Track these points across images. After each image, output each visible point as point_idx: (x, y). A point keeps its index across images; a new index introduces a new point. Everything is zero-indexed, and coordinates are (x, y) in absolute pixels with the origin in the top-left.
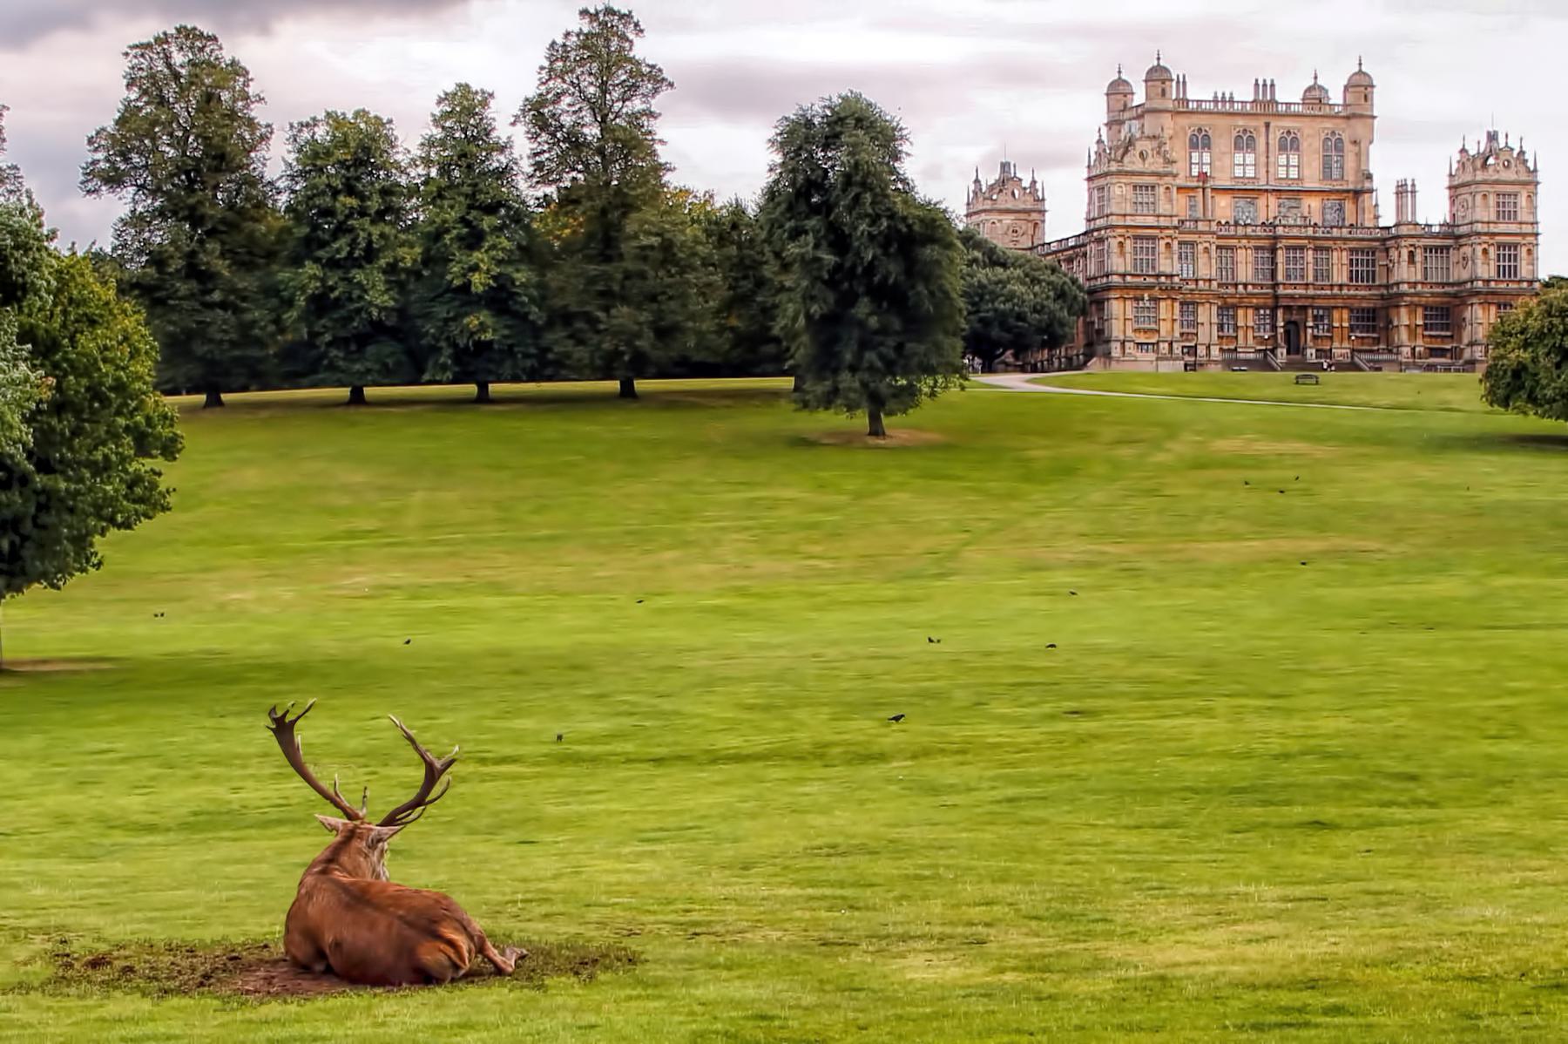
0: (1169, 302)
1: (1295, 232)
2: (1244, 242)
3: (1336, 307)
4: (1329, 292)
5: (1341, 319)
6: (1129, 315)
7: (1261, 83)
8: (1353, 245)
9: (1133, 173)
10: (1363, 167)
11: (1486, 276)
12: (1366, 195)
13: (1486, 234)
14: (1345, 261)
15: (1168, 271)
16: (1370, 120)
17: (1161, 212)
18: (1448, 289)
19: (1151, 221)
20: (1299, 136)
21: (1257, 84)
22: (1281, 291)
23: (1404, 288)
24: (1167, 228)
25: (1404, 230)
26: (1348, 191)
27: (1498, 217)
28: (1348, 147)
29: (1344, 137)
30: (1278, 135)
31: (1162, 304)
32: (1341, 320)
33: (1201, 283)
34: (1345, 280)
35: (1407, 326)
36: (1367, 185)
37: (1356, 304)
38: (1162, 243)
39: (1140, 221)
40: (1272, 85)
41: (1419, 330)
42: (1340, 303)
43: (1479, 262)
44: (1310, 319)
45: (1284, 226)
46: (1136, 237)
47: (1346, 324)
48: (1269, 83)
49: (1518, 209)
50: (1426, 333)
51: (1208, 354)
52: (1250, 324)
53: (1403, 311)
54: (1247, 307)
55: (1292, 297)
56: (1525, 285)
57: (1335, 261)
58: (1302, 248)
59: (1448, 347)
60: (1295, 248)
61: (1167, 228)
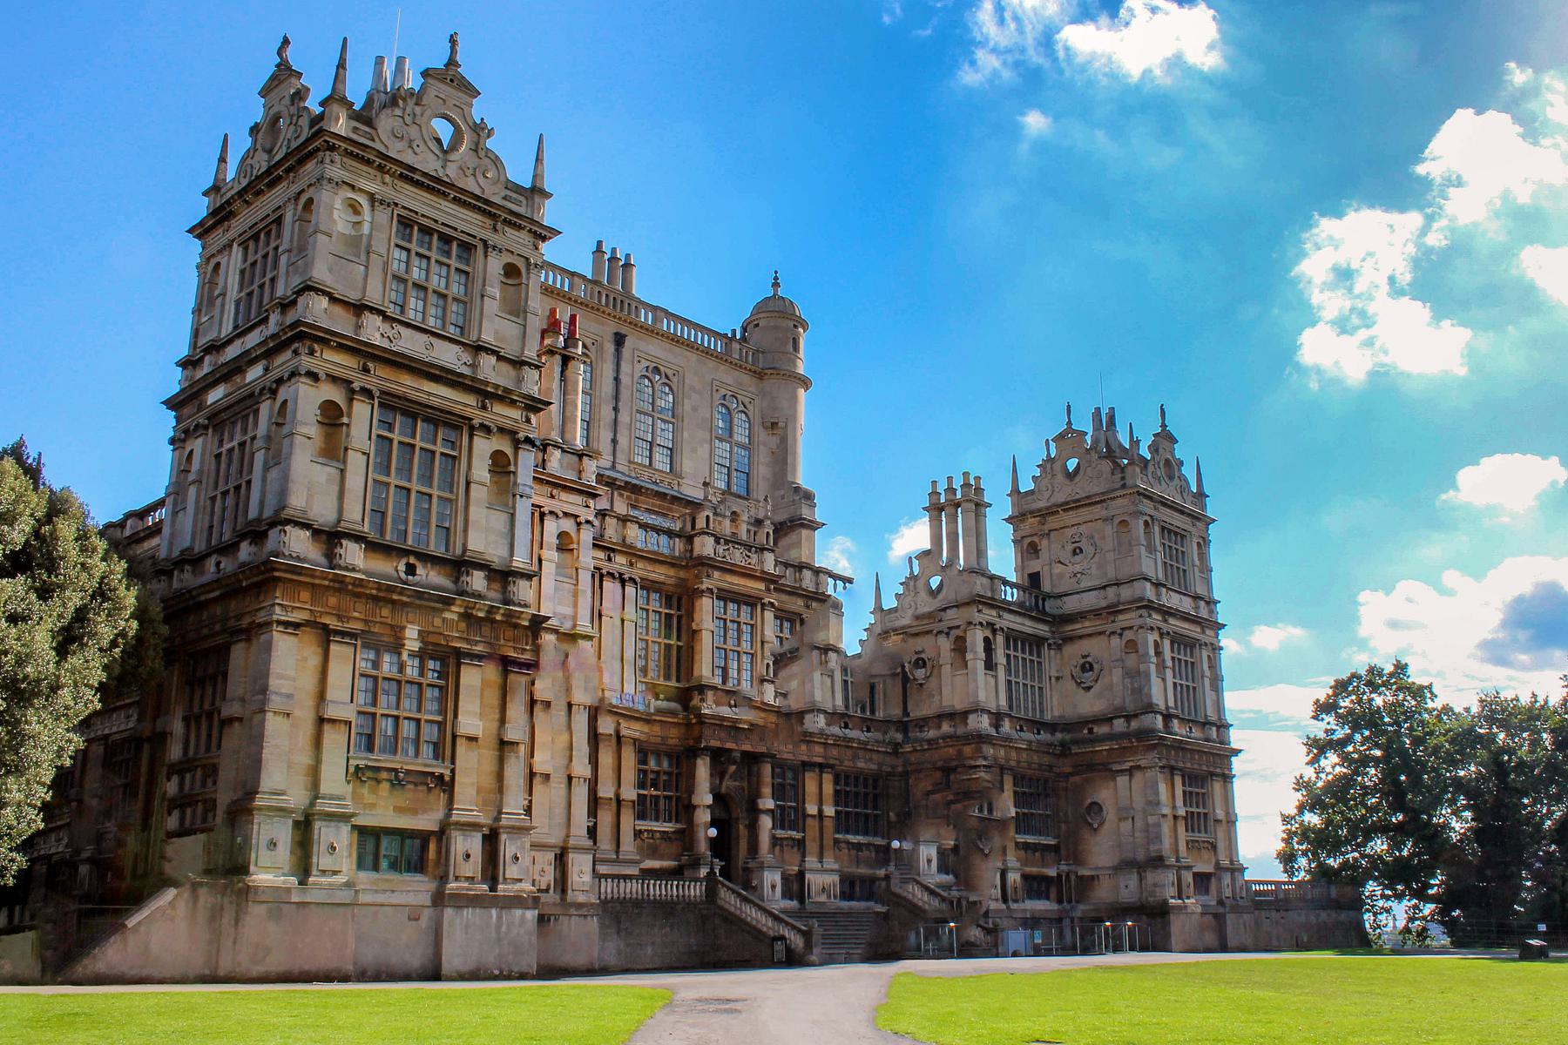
5: (819, 797)
6: (341, 706)
9: (409, 175)
12: (805, 532)
15: (495, 553)
17: (488, 337)
19: (449, 356)
24: (505, 397)
38: (484, 447)
39: (410, 344)
40: (628, 266)
44: (767, 790)
46: (392, 404)
47: (829, 811)
50: (1021, 839)
55: (733, 728)
58: (752, 601)
59: (1052, 872)
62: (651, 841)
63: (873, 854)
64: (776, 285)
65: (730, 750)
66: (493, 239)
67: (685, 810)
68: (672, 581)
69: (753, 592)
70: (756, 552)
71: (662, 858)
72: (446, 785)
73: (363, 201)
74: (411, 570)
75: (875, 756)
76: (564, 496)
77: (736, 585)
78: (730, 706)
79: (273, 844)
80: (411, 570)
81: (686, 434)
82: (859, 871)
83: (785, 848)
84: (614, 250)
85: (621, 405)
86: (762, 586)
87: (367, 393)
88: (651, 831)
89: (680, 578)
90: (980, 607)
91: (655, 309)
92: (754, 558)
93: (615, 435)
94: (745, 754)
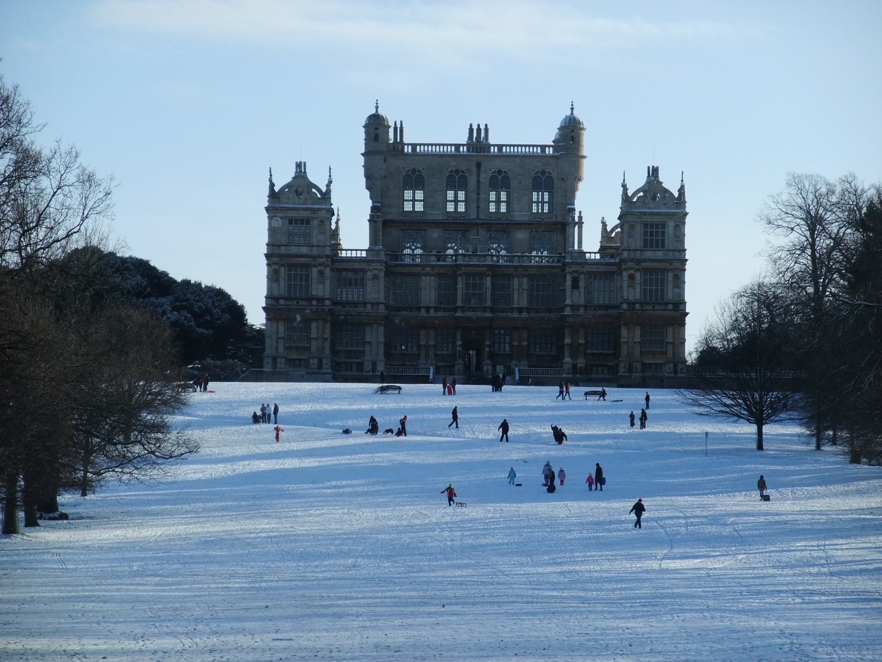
0: (320, 323)
7: (475, 127)
11: (632, 298)
13: (632, 260)
14: (525, 286)
15: (320, 294)
18: (610, 311)
19: (304, 250)
21: (471, 130)
22: (459, 314)
23: (567, 312)
24: (320, 257)
27: (645, 246)
29: (554, 175)
30: (490, 174)
31: (314, 325)
33: (369, 306)
34: (524, 303)
35: (570, 345)
38: (315, 270)
39: (294, 250)
40: (486, 129)
43: (625, 285)
48: (482, 127)
49: (666, 238)
52: (432, 343)
53: (567, 331)
56: (670, 307)
61: (320, 257)
66: (314, 216)
67: (454, 346)
72: (309, 349)
73: (279, 219)
74: (298, 302)
79: (268, 363)
80: (298, 302)
81: (515, 195)
84: (479, 125)
87: (283, 265)
92: (482, 259)
93: (478, 203)
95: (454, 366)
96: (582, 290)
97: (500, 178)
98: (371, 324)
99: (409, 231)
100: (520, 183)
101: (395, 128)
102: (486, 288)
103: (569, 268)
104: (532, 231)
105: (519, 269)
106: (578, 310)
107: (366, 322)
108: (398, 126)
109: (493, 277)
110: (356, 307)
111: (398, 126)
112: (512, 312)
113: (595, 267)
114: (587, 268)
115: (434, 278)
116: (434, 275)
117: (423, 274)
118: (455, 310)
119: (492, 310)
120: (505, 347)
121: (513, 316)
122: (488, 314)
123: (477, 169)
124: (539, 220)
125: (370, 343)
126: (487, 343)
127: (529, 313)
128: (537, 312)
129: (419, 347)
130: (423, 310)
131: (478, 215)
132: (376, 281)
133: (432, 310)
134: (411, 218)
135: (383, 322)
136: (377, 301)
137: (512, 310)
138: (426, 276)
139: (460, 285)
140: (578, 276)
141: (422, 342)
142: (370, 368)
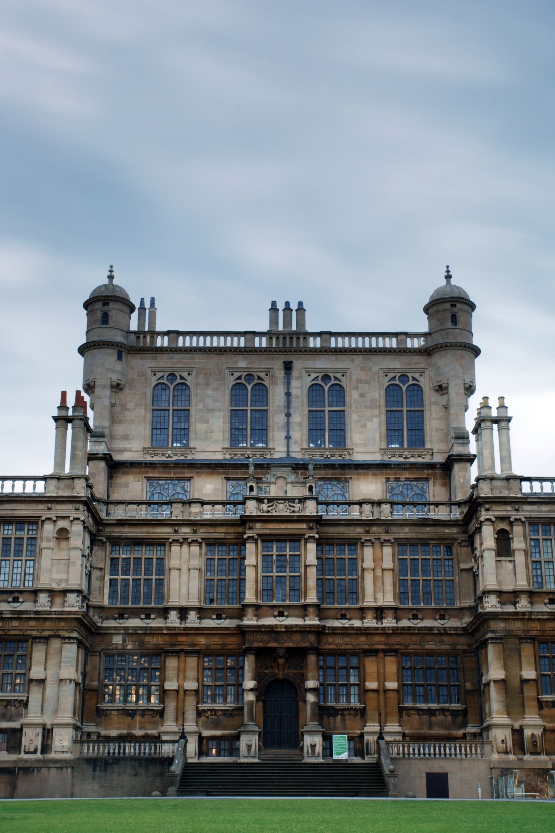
1: (282, 510)
2: (185, 531)
3: (373, 652)
4: (357, 623)
7: (281, 306)
8: (405, 532)
10: (454, 425)
14: (388, 563)
16: (468, 354)
20: (344, 382)
21: (274, 309)
22: (249, 621)
25: (485, 491)
26: (431, 466)
28: (429, 396)
30: (308, 381)
32: (382, 678)
36: (458, 450)
37: (413, 643)
40: (301, 309)
41: (530, 692)
42: (379, 642)
45: (260, 500)
47: (392, 685)
48: (294, 306)
51: (46, 748)
53: (492, 651)
54: (188, 653)
55: (271, 630)
57: (368, 563)
60: (281, 539)
62: (214, 717)
63: (449, 718)
64: (448, 277)
65: (274, 649)
68: (232, 536)
69: (298, 532)
70: (299, 503)
71: (224, 728)
75: (446, 639)
76: (59, 507)
77: (277, 529)
78: (275, 617)
81: (355, 417)
82: (432, 732)
83: (347, 717)
84: (287, 304)
85: (292, 411)
86: (304, 526)
88: (215, 710)
89: (238, 533)
90: (487, 506)
91: (320, 334)
92: (298, 506)
93: (288, 431)
94: (288, 649)
95: (237, 737)
96: (520, 558)
97: (326, 388)
98: (46, 640)
99: (161, 482)
100: (362, 395)
101: (142, 308)
102: (306, 566)
103: (487, 510)
104: (388, 480)
105: (374, 529)
106: (514, 604)
107: (34, 633)
108: (147, 305)
109: (320, 543)
110: (16, 600)
111: (147, 305)
112: (362, 618)
113: (544, 508)
114: (528, 510)
115: (198, 548)
116: (197, 541)
117: (174, 541)
118: (240, 613)
119: (321, 612)
120: (348, 695)
121: (366, 625)
122: (312, 621)
123: (286, 374)
124: (401, 459)
125: (42, 682)
126: (311, 684)
127: (397, 619)
128: (415, 617)
129: (163, 694)
130: (173, 615)
131: (288, 452)
132: (64, 544)
133: (193, 616)
134: (164, 459)
135: (75, 635)
136: (63, 586)
137: (362, 611)
138: (181, 544)
139: (250, 560)
140: (507, 528)
141: (171, 685)
142: (38, 742)
